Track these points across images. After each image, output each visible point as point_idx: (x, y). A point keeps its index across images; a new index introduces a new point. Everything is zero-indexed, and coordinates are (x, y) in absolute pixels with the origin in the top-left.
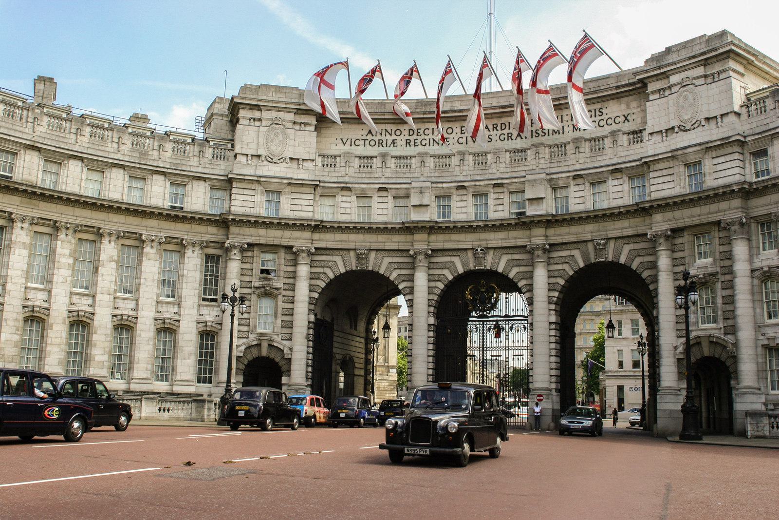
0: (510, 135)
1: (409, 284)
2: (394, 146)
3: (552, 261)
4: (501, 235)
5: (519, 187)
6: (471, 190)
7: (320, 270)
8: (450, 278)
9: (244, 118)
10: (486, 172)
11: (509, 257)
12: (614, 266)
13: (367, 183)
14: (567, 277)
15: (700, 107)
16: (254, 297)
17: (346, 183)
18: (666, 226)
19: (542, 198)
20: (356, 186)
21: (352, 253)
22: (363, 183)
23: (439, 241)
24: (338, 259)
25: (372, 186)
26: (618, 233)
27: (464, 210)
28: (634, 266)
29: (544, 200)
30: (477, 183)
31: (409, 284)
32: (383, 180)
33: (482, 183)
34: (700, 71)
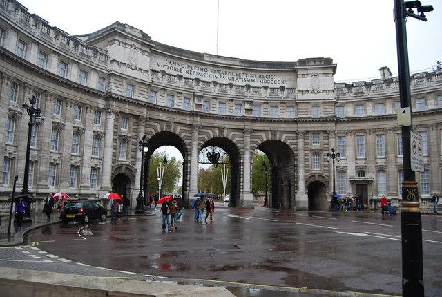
1: (190, 141)
4: (233, 123)
5: (240, 103)
7: (149, 129)
9: (117, 40)
11: (233, 133)
12: (279, 142)
16: (118, 140)
18: (304, 129)
21: (164, 123)
23: (207, 122)
24: (157, 125)
26: (282, 129)
28: (287, 143)
31: (190, 141)
34: (321, 71)
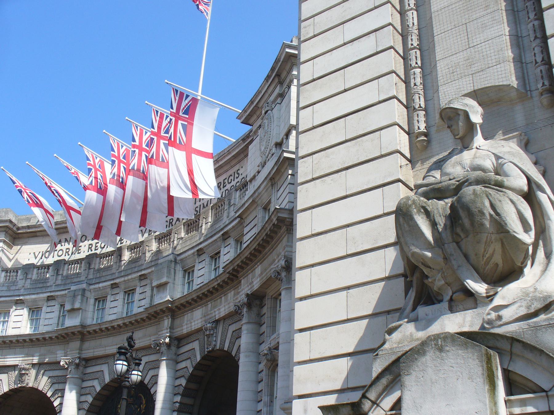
0: (171, 221)
2: (78, 253)
3: (180, 358)
6: (122, 286)
8: (98, 389)
10: (137, 264)
13: (37, 293)
14: (187, 375)
15: (271, 133)
17: (19, 296)
19: (166, 284)
20: (28, 297)
22: (34, 294)
25: (42, 296)
27: (115, 311)
29: (168, 285)
30: (126, 278)
32: (53, 288)
33: (130, 277)
